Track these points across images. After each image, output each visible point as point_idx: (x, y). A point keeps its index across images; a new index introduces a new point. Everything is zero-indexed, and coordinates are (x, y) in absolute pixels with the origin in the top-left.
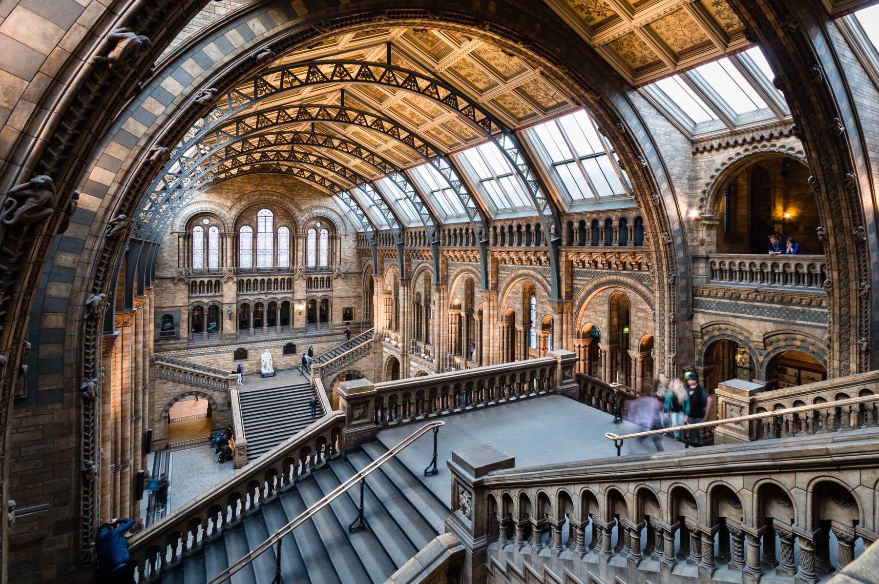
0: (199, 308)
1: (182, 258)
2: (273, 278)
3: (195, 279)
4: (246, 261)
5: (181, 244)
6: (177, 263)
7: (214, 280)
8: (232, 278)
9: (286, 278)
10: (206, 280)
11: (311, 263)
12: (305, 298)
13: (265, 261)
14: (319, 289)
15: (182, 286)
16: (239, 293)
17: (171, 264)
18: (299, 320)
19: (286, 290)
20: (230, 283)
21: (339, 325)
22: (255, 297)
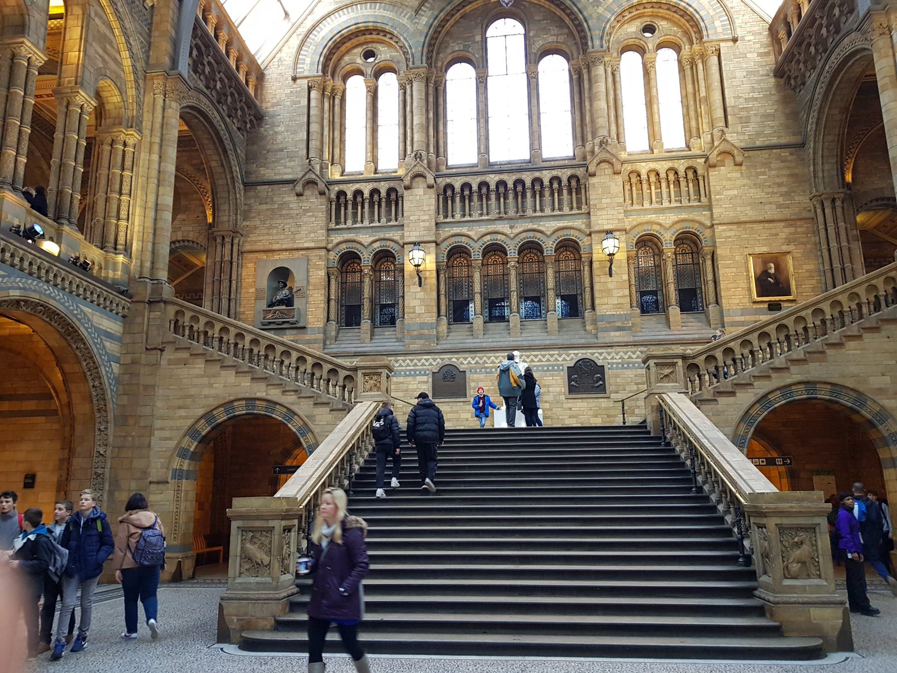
0: (349, 259)
2: (528, 178)
3: (342, 187)
5: (313, 103)
6: (304, 145)
7: (383, 187)
8: (425, 177)
9: (564, 174)
10: (366, 189)
12: (620, 226)
16: (441, 219)
17: (291, 148)
18: (608, 292)
19: (566, 210)
21: (744, 312)
22: (483, 229)
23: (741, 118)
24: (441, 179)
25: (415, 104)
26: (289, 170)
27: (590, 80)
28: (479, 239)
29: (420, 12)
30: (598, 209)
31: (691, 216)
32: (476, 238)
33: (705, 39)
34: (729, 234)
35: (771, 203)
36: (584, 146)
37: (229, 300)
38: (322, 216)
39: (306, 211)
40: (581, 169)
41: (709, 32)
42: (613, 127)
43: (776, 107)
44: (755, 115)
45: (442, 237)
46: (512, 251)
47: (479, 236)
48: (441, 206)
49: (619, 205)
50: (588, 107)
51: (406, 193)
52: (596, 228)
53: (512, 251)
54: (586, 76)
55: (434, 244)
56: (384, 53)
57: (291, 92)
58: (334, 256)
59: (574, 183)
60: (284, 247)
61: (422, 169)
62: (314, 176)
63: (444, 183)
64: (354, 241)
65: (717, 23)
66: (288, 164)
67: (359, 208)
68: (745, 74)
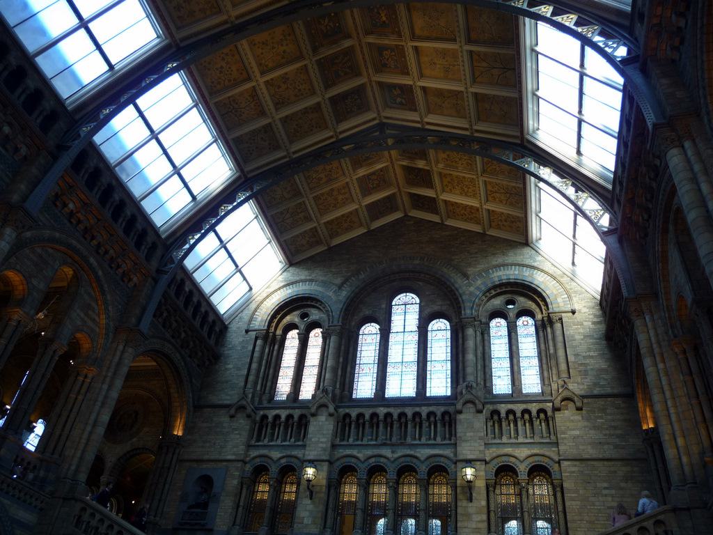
1: (253, 372)
2: (409, 412)
3: (267, 412)
4: (364, 387)
5: (257, 349)
6: (243, 379)
9: (439, 410)
11: (501, 385)
12: (481, 456)
13: (401, 385)
14: (521, 440)
15: (242, 423)
16: (338, 441)
18: (468, 516)
19: (439, 440)
20: (322, 418)
22: (369, 452)
23: (580, 371)
24: (341, 410)
25: (330, 352)
26: (228, 398)
27: (463, 338)
28: (365, 460)
29: (343, 288)
30: (463, 441)
31: (541, 452)
32: (362, 460)
33: (551, 310)
34: (573, 469)
35: (608, 444)
36: (456, 388)
37: (160, 500)
38: (245, 434)
39: (236, 429)
40: (452, 407)
41: (554, 306)
42: (480, 374)
43: (608, 363)
44: (592, 369)
45: (336, 457)
46: (392, 473)
47: (365, 458)
48: (339, 430)
49: (480, 438)
50: (461, 359)
51: (312, 419)
52: (461, 457)
53: (392, 473)
54: (460, 335)
55: (327, 463)
56: (315, 315)
57: (243, 341)
58: (248, 468)
59: (447, 418)
60: (212, 457)
61: (326, 401)
62: (245, 403)
63: (343, 413)
64: (266, 456)
65: (559, 300)
66: (229, 393)
67: (277, 429)
68: (582, 337)
